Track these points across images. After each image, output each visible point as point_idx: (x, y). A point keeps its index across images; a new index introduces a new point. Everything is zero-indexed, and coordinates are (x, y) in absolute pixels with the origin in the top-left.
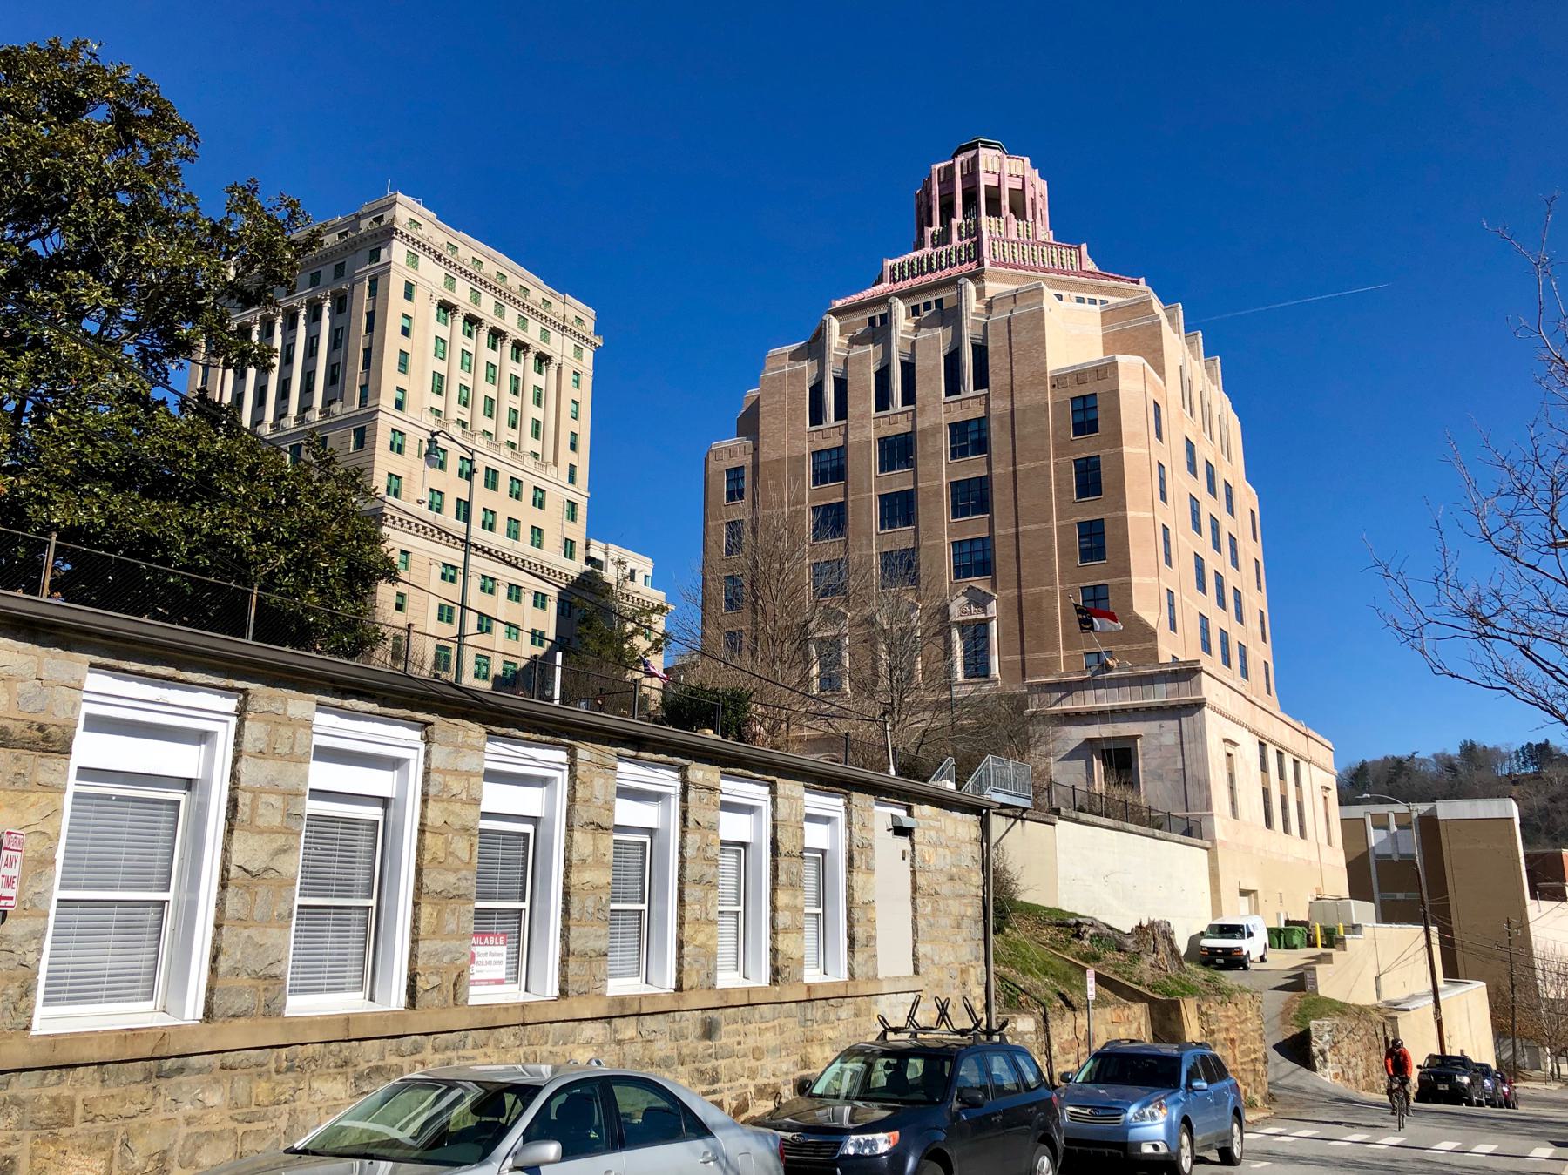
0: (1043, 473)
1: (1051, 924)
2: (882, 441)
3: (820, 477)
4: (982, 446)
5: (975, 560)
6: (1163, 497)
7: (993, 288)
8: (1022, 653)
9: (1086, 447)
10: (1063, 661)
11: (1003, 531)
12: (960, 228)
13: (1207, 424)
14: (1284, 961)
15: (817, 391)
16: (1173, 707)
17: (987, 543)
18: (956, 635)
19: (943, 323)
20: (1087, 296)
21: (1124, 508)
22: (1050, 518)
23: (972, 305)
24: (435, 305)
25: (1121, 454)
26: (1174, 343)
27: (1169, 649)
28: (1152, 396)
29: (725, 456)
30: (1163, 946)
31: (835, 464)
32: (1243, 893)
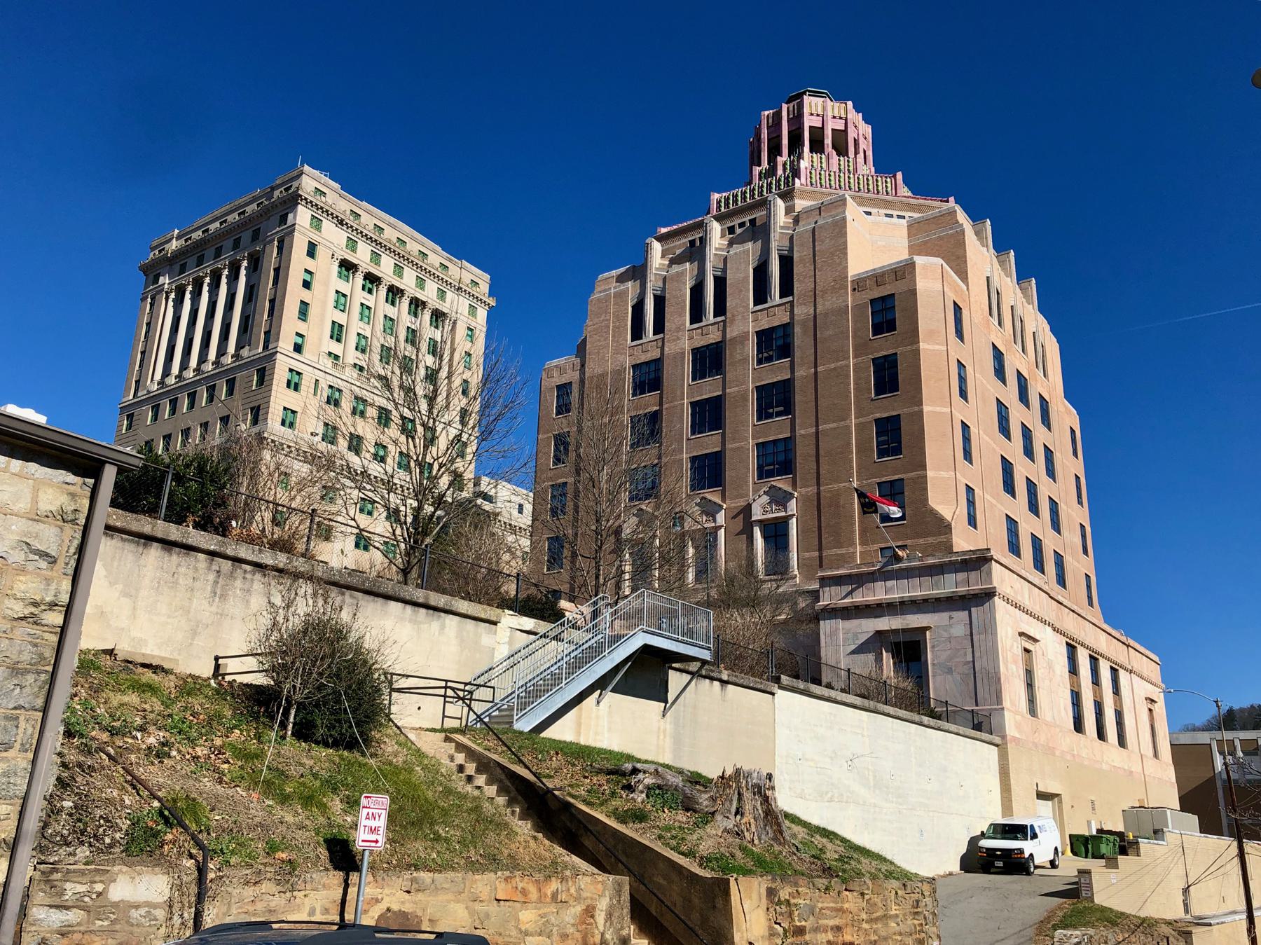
0: (842, 373)
1: (600, 771)
4: (786, 350)
5: (777, 460)
6: (963, 394)
8: (820, 550)
9: (884, 346)
10: (859, 555)
11: (804, 431)
12: (784, 165)
13: (1019, 334)
15: (638, 309)
16: (963, 597)
17: (788, 443)
18: (757, 532)
19: (754, 239)
20: (895, 213)
21: (920, 403)
25: (917, 352)
26: (980, 254)
27: (963, 541)
28: (951, 296)
30: (751, 804)
31: (652, 376)
32: (1042, 796)
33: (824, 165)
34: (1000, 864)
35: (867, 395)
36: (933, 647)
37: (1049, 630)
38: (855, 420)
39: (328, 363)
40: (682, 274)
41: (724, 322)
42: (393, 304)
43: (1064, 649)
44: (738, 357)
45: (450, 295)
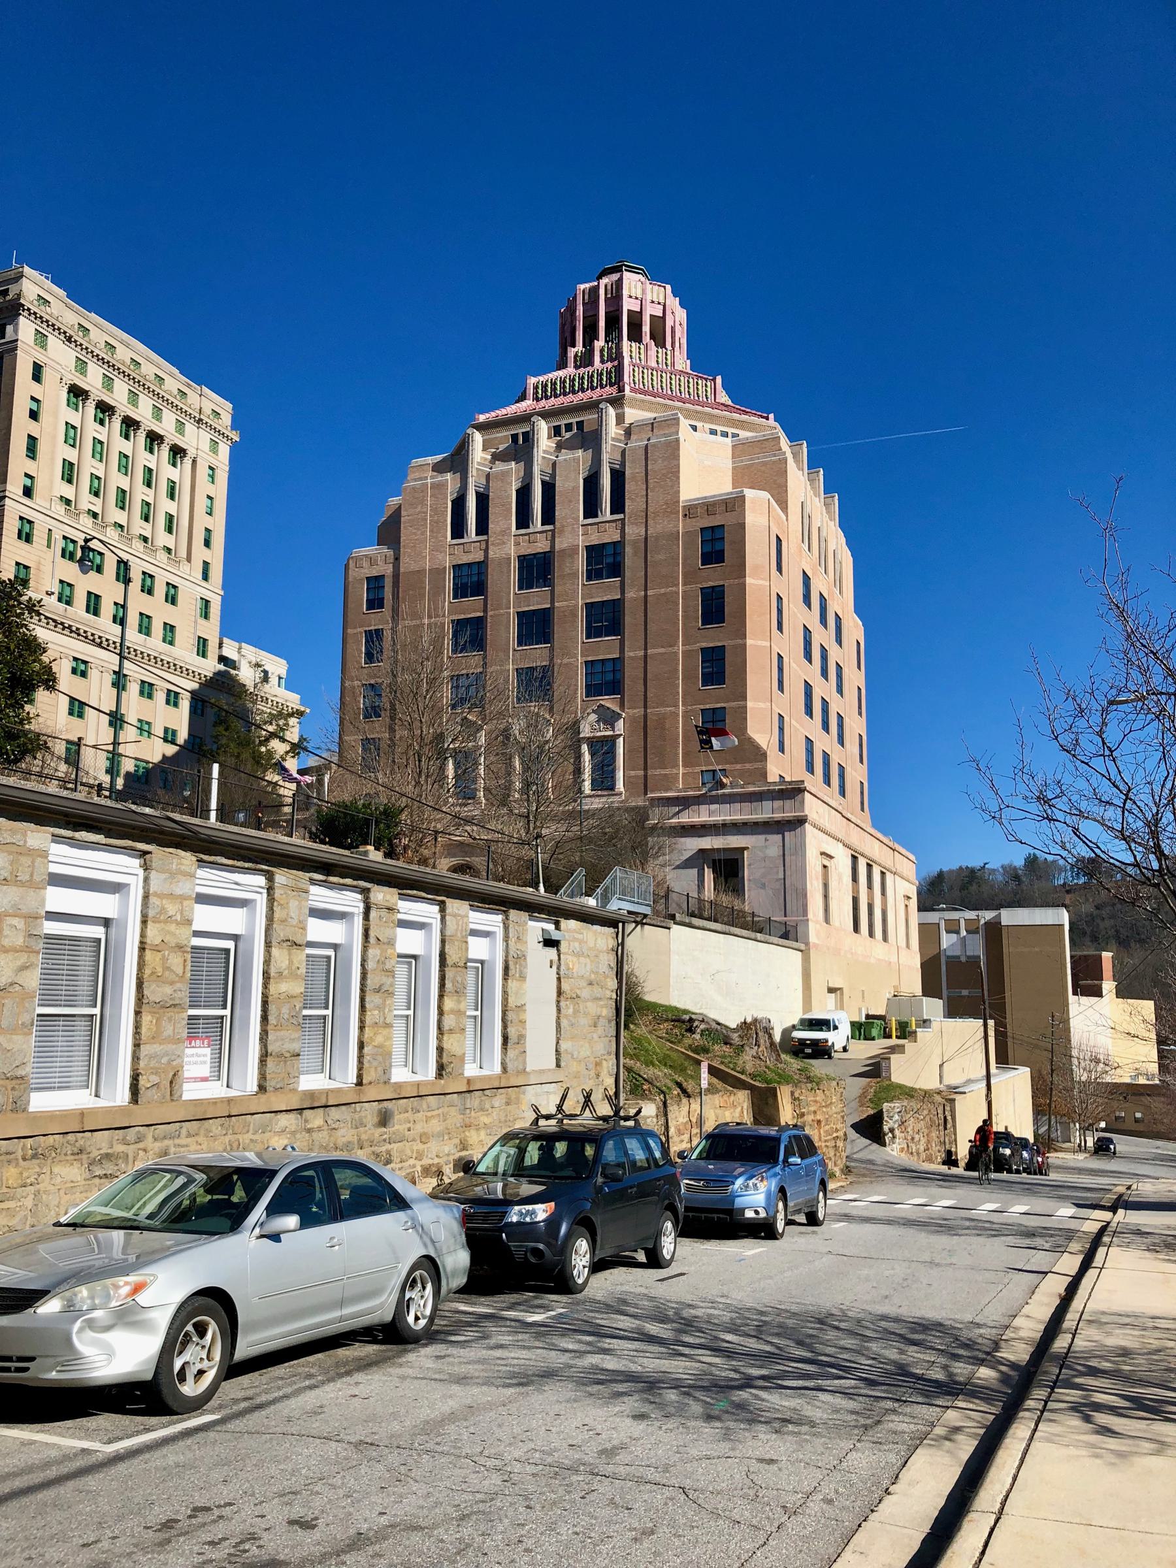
0: (671, 600)
1: (667, 1020)
2: (522, 559)
3: (461, 591)
4: (616, 569)
5: (605, 680)
7: (633, 415)
8: (645, 769)
9: (713, 576)
11: (633, 653)
12: (602, 351)
14: (864, 1051)
15: (459, 504)
16: (778, 822)
17: (617, 664)
18: (585, 748)
19: (583, 446)
20: (719, 428)
22: (676, 643)
23: (612, 430)
24: (65, 390)
25: (744, 584)
26: (801, 483)
27: (778, 769)
28: (775, 530)
29: (365, 564)
31: (475, 579)
32: (831, 990)
33: (642, 357)
34: (809, 1051)
35: (694, 624)
36: (749, 865)
37: (841, 845)
38: (682, 649)
39: (59, 509)
40: (509, 472)
41: (553, 531)
42: (127, 437)
43: (848, 862)
44: (567, 571)
45: (190, 428)
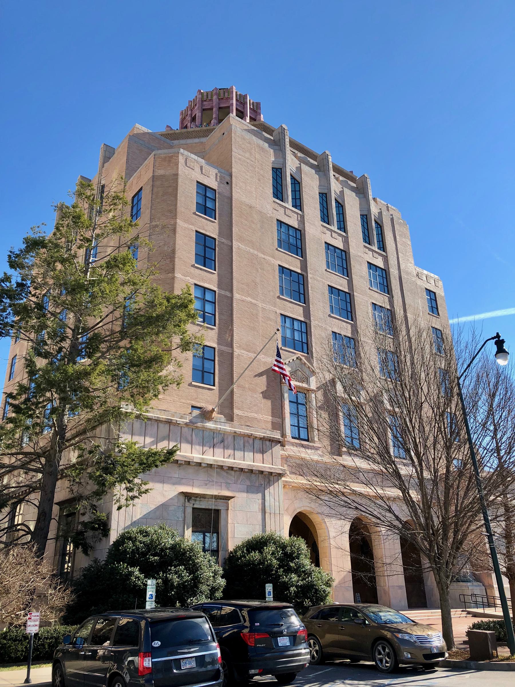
29: (198, 169)
